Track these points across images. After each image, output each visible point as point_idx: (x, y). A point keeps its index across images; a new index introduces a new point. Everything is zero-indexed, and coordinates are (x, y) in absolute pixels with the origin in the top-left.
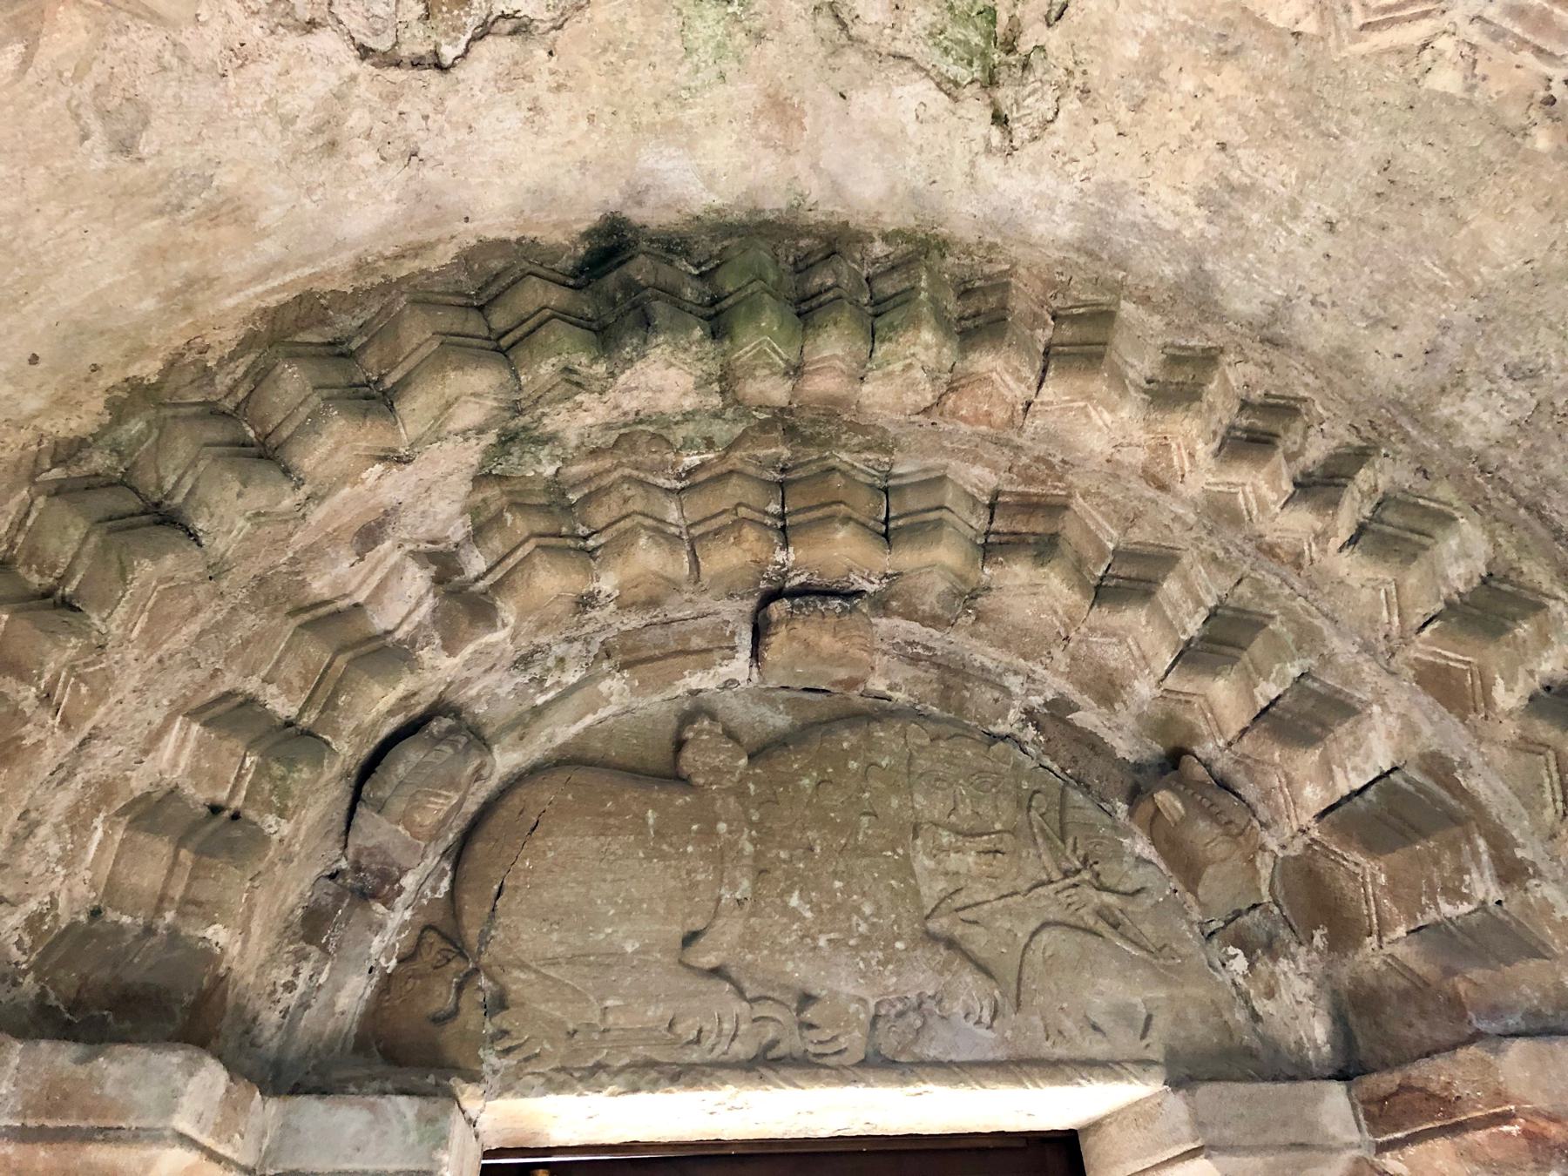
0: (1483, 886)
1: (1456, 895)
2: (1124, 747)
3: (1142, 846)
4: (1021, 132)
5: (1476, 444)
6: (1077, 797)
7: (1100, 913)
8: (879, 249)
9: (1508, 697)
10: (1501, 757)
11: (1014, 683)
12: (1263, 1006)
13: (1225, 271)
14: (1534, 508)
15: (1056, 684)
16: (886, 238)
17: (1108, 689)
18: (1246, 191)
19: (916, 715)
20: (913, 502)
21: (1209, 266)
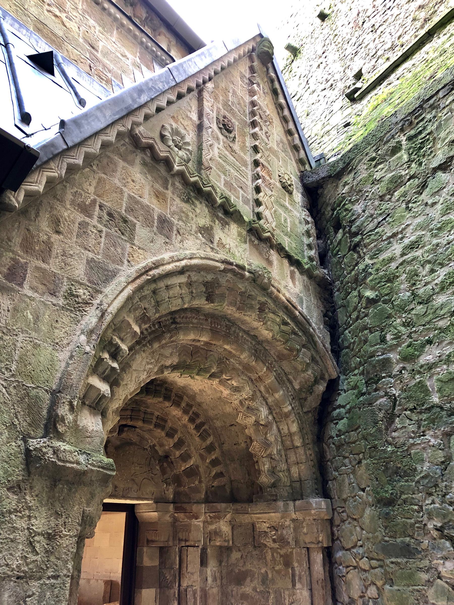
0: (197, 482)
1: (194, 484)
2: (160, 453)
3: (158, 467)
4: (183, 376)
5: (216, 426)
6: (152, 459)
7: (152, 477)
9: (208, 461)
10: (205, 467)
11: (149, 441)
12: (166, 492)
13: (198, 397)
14: (219, 436)
15: (155, 442)
17: (162, 445)
18: (205, 391)
19: (135, 444)
20: (149, 416)
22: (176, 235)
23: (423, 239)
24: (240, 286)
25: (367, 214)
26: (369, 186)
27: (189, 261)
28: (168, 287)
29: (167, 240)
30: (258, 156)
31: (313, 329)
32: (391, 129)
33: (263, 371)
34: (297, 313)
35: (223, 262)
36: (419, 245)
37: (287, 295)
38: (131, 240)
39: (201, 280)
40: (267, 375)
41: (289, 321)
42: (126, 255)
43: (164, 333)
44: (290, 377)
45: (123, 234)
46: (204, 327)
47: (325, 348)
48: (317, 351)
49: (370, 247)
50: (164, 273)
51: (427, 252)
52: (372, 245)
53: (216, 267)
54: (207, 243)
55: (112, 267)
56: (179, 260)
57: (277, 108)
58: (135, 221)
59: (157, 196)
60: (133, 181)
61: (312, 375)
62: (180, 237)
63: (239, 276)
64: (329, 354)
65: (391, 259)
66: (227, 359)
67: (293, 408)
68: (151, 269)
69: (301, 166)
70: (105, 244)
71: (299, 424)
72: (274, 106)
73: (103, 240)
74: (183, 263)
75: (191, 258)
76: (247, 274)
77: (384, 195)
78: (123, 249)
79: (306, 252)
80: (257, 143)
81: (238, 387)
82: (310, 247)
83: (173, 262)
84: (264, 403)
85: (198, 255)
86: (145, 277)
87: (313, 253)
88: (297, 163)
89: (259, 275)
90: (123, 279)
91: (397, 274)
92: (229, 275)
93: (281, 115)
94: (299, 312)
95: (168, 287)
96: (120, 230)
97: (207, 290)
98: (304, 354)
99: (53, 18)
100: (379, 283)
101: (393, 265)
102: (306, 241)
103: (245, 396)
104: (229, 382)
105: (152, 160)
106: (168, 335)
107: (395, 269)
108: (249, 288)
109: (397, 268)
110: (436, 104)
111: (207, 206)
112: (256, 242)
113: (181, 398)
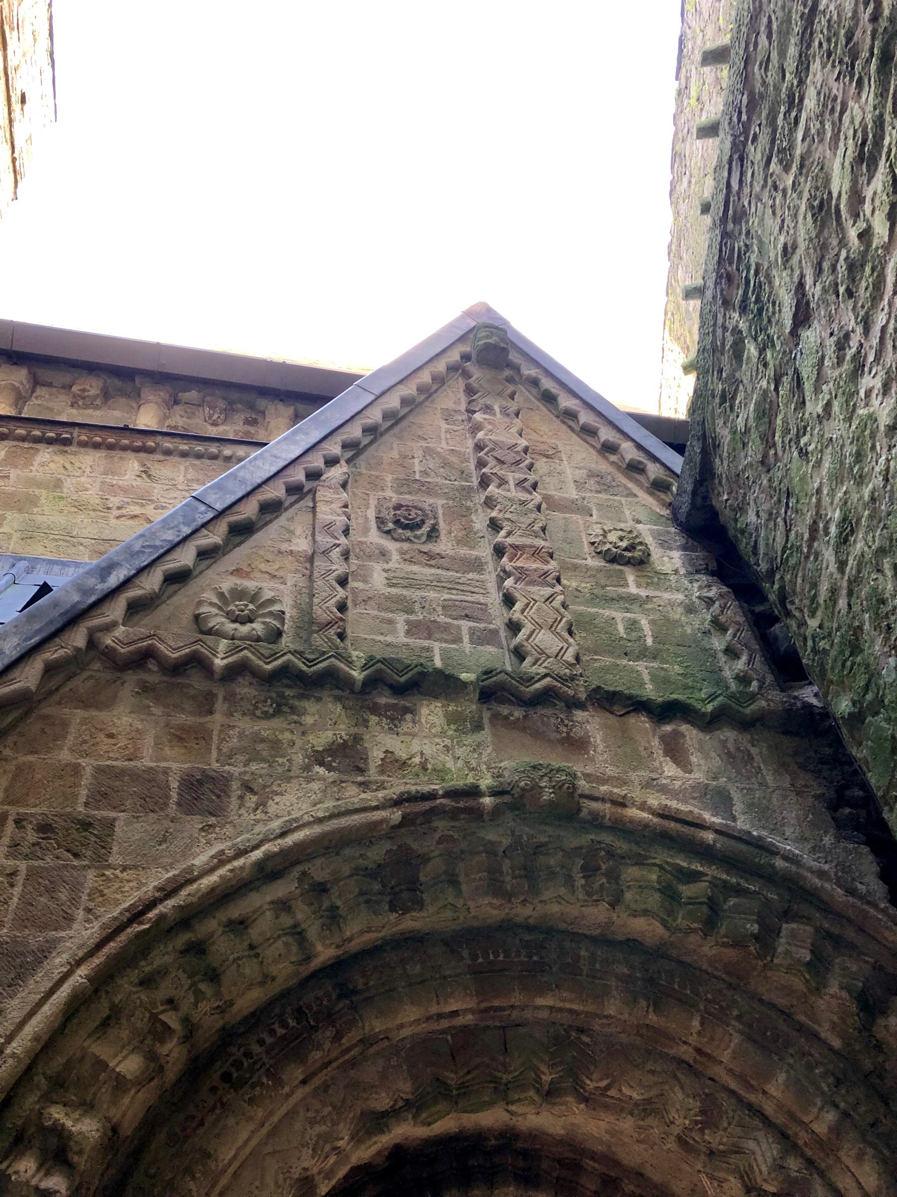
8: (493, 1142)
16: (495, 1138)
21: (614, 1149)
22: (241, 798)
23: (849, 503)
24: (491, 836)
25: (764, 516)
26: (743, 454)
27: (279, 841)
28: (240, 926)
29: (212, 820)
30: (500, 537)
31: (786, 858)
32: (715, 317)
33: (694, 1031)
34: (709, 837)
35: (397, 803)
36: (851, 523)
37: (655, 800)
38: (100, 861)
39: (346, 870)
40: (712, 1039)
41: (697, 867)
42: (85, 897)
43: (315, 1029)
44: (802, 1018)
45: (76, 855)
46: (447, 973)
47: (861, 898)
48: (839, 916)
49: (798, 589)
50: (194, 899)
51: (870, 529)
52: (799, 580)
53: (376, 824)
54: (345, 778)
55: (36, 939)
56: (242, 853)
57: (564, 423)
58: (113, 814)
59: (181, 739)
60: (111, 736)
61: (844, 994)
62: (254, 798)
63: (462, 816)
64: (883, 911)
65: (834, 592)
66: (581, 1031)
67: (846, 1115)
68: (152, 904)
69: (663, 496)
70: (22, 897)
71: (884, 1161)
72: (558, 422)
73: (17, 890)
74: (257, 854)
75: (283, 835)
76: (487, 801)
77: (765, 456)
78: (76, 888)
79: (727, 668)
80: (494, 514)
81: (648, 1101)
82: (731, 653)
83: (221, 863)
84: (757, 1122)
85: (306, 818)
86: (137, 928)
87: (740, 664)
88: (651, 494)
89: (523, 789)
90: (65, 956)
91: (857, 624)
92: (441, 825)
93: (577, 429)
94: (717, 832)
95: (240, 926)
96: (68, 851)
97: (384, 886)
98: (793, 935)
99: (131, 522)
100: (843, 665)
101: (842, 603)
102: (718, 643)
103: (681, 1122)
104: (612, 1093)
105: (165, 674)
106: (328, 1033)
107: (848, 613)
108: (525, 831)
109: (849, 605)
110: (739, 209)
111: (338, 699)
112: (518, 713)
113: (575, 1167)
